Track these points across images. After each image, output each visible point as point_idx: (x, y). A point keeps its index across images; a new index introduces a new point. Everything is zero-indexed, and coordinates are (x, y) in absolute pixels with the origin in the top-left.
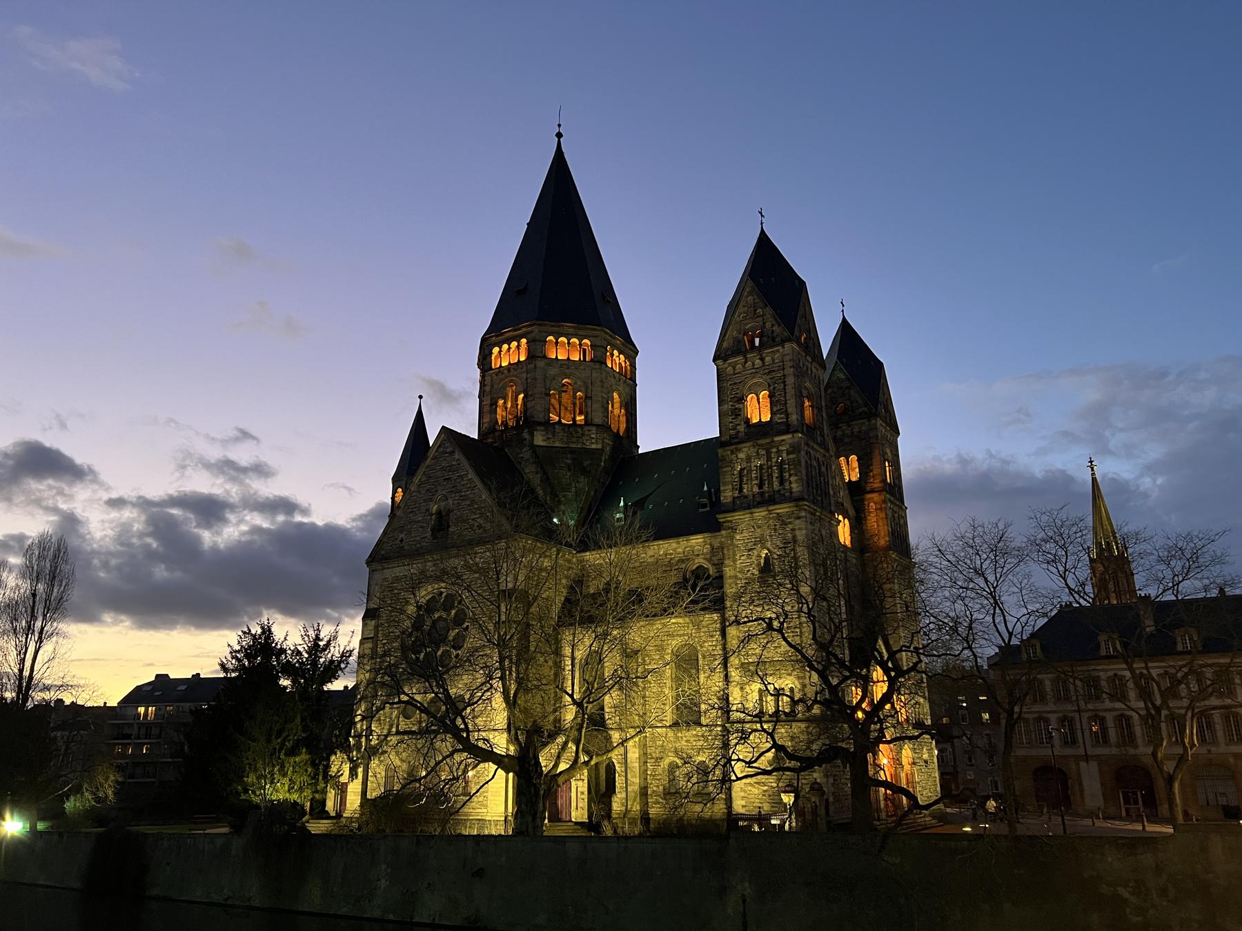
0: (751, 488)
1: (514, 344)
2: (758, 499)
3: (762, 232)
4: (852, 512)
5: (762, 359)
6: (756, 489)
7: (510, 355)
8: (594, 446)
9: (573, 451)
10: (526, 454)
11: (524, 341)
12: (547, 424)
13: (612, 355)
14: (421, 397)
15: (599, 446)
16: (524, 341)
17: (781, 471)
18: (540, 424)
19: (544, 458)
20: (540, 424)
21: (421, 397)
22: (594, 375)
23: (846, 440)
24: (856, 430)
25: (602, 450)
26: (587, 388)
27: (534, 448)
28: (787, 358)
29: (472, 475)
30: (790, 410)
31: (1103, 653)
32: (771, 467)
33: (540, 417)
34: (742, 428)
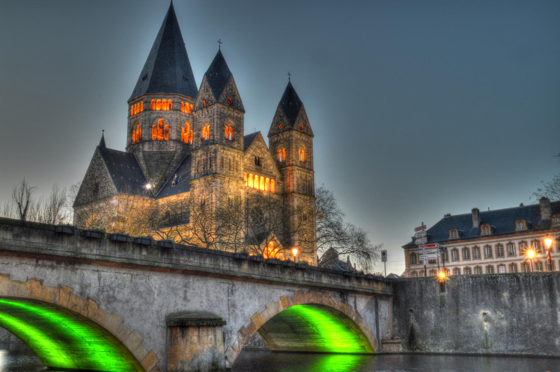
0: (201, 169)
1: (139, 104)
2: (203, 174)
3: (219, 51)
4: (278, 176)
5: (208, 111)
6: (202, 170)
7: (138, 108)
8: (171, 150)
9: (161, 153)
10: (141, 155)
11: (142, 102)
12: (150, 141)
13: (185, 105)
14: (103, 131)
15: (174, 150)
16: (142, 102)
17: (211, 161)
18: (146, 141)
19: (148, 157)
20: (146, 141)
21: (103, 131)
22: (173, 116)
23: (282, 142)
24: (285, 136)
25: (176, 151)
26: (170, 123)
27: (144, 152)
28: (216, 110)
29: (106, 168)
30: (215, 134)
31: (450, 238)
32: (207, 160)
33: (146, 138)
34: (200, 143)
